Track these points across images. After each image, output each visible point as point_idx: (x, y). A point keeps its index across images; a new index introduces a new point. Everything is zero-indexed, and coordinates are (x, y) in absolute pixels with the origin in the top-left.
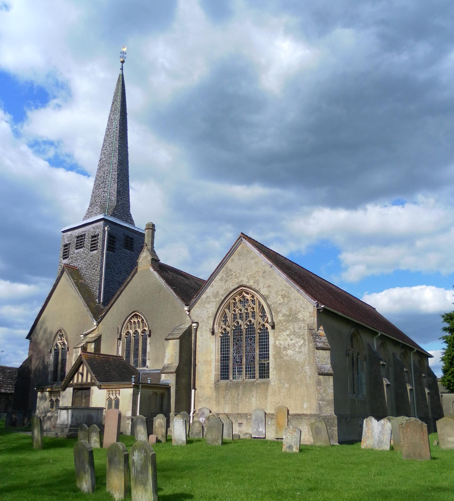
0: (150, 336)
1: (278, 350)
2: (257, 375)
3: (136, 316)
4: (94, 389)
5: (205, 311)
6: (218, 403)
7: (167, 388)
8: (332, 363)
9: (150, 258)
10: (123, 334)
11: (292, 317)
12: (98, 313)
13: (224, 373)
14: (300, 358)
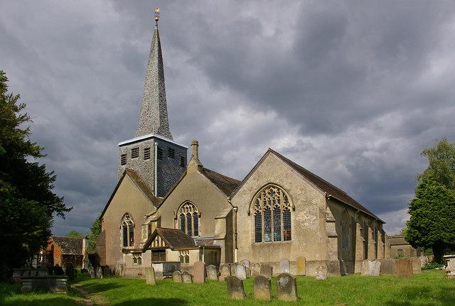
0: (200, 216)
1: (298, 223)
2: (282, 239)
3: (188, 204)
4: (168, 251)
5: (242, 199)
6: (254, 256)
7: (219, 249)
8: (336, 230)
9: (196, 165)
10: (179, 216)
11: (308, 202)
12: (158, 204)
13: (258, 238)
14: (314, 228)
